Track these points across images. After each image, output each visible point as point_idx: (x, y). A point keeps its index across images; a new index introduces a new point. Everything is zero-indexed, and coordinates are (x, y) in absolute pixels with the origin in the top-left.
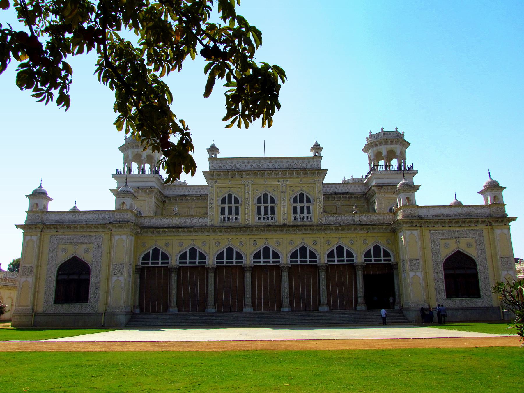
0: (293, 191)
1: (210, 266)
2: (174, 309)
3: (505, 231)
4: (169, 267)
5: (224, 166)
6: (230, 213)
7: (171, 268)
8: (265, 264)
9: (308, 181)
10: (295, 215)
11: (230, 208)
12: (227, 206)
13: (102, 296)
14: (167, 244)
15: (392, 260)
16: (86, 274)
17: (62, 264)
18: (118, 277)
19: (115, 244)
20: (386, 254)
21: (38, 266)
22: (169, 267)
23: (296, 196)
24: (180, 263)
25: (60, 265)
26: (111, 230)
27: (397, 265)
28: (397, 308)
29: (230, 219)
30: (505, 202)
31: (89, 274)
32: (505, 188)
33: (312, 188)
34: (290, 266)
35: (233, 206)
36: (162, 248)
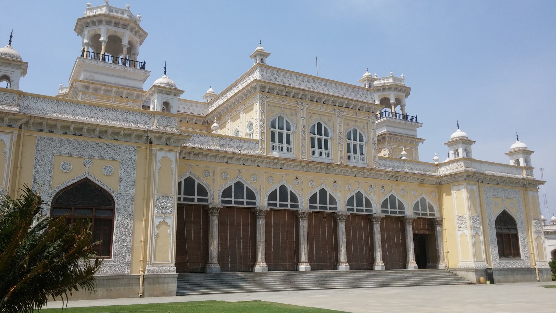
0: (348, 125)
1: (264, 209)
2: (214, 266)
3: (535, 193)
4: (211, 206)
5: (276, 78)
6: (281, 141)
7: (213, 208)
8: (322, 211)
9: (362, 116)
10: (349, 154)
11: (281, 135)
14: (206, 174)
15: (436, 215)
17: (61, 191)
20: (431, 209)
22: (211, 206)
23: (350, 132)
24: (223, 202)
25: (57, 191)
26: (151, 143)
27: (442, 221)
28: (441, 266)
30: (533, 166)
31: (113, 210)
32: (533, 152)
33: (366, 125)
34: (349, 214)
35: (285, 132)
36: (199, 179)
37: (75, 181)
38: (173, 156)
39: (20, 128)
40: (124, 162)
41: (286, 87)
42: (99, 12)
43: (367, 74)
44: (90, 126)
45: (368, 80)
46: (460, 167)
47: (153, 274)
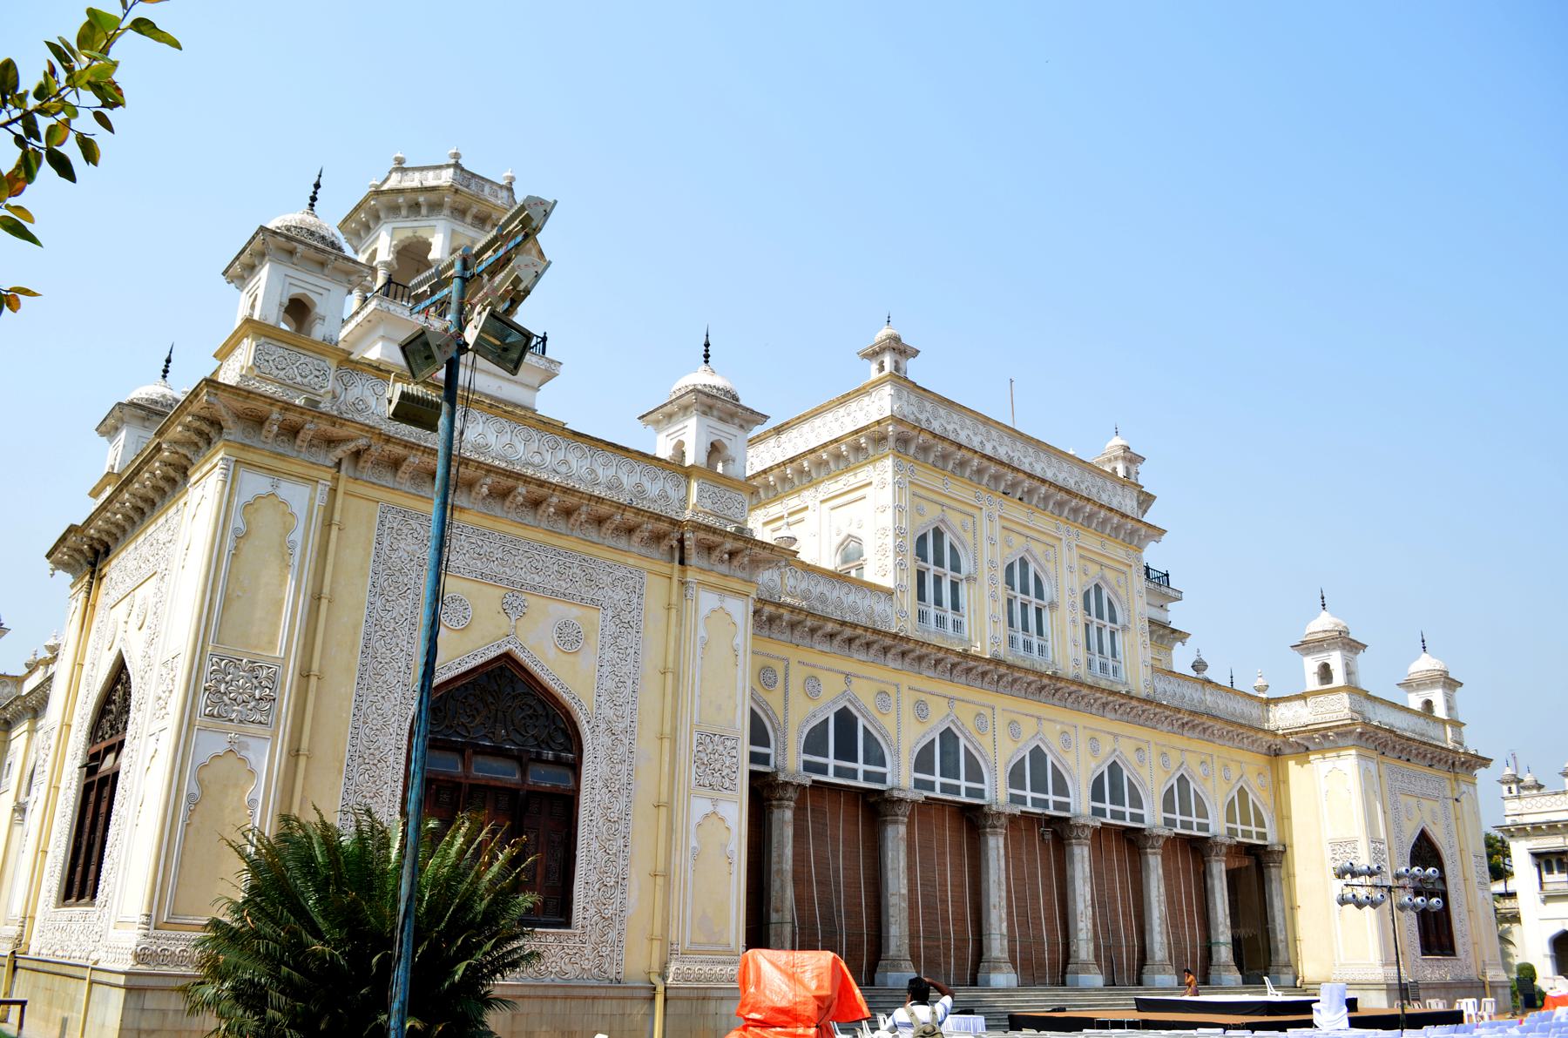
4: (782, 777)
12: (932, 570)
13: (638, 897)
16: (558, 762)
18: (715, 801)
19: (702, 632)
21: (305, 675)
22: (782, 777)
29: (940, 621)
31: (575, 767)
33: (1122, 577)
37: (479, 661)
38: (740, 610)
39: (338, 464)
40: (610, 614)
41: (960, 446)
42: (431, 179)
43: (1118, 441)
44: (533, 488)
45: (1124, 458)
46: (1337, 709)
47: (688, 985)
